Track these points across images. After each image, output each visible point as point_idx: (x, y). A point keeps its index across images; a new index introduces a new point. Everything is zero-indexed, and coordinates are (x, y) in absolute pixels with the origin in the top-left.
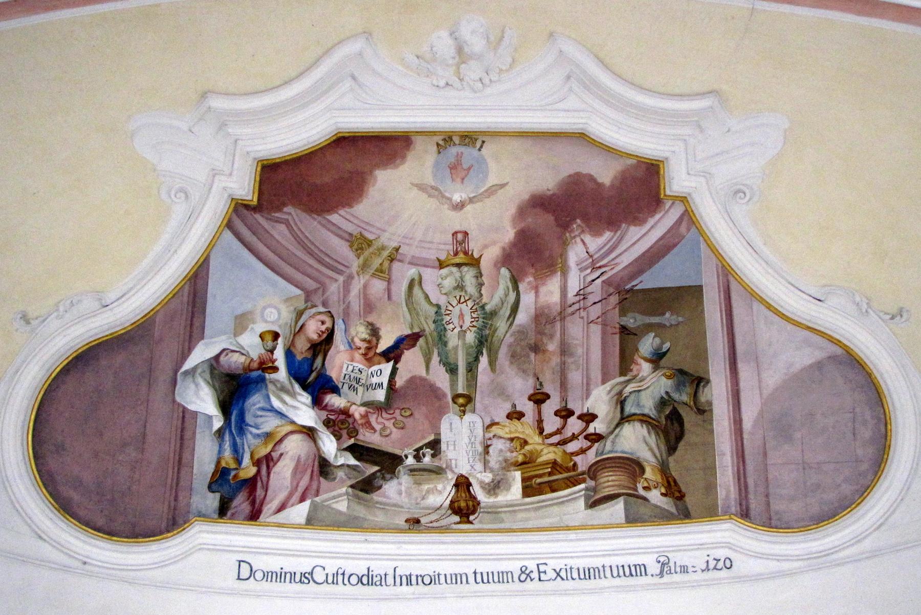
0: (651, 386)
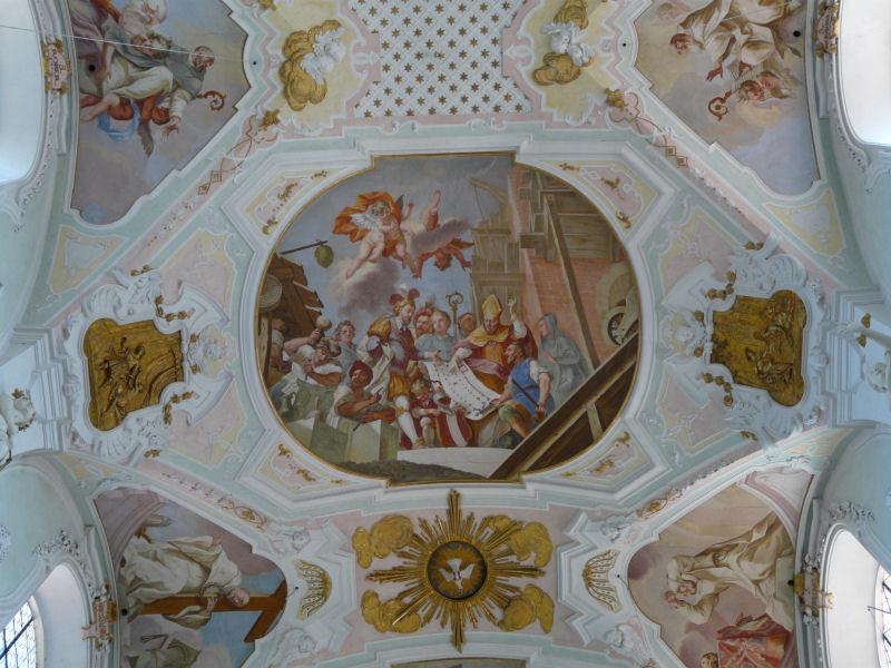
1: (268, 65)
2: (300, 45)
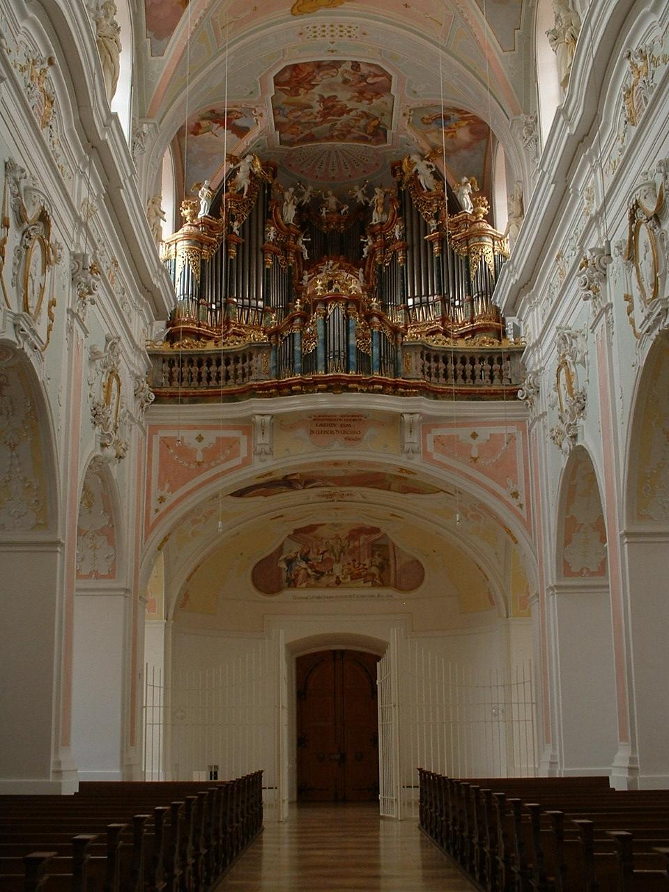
0: (378, 560)
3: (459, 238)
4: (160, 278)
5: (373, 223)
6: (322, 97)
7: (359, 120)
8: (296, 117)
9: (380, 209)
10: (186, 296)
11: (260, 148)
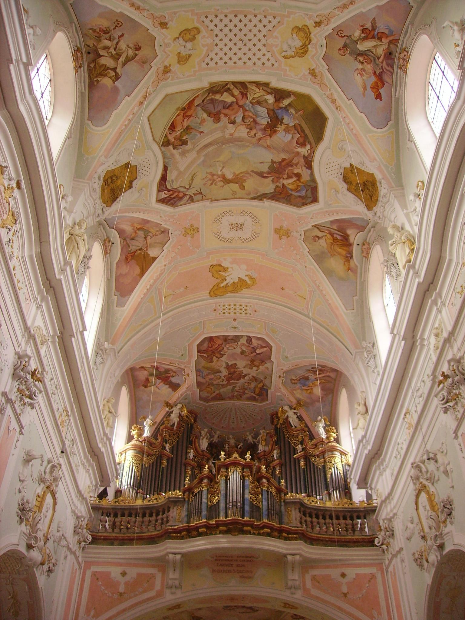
1: (316, 44)
2: (301, 51)
3: (318, 453)
4: (104, 444)
5: (259, 451)
6: (227, 364)
7: (250, 383)
8: (210, 379)
9: (264, 443)
10: (129, 486)
11: (187, 401)
